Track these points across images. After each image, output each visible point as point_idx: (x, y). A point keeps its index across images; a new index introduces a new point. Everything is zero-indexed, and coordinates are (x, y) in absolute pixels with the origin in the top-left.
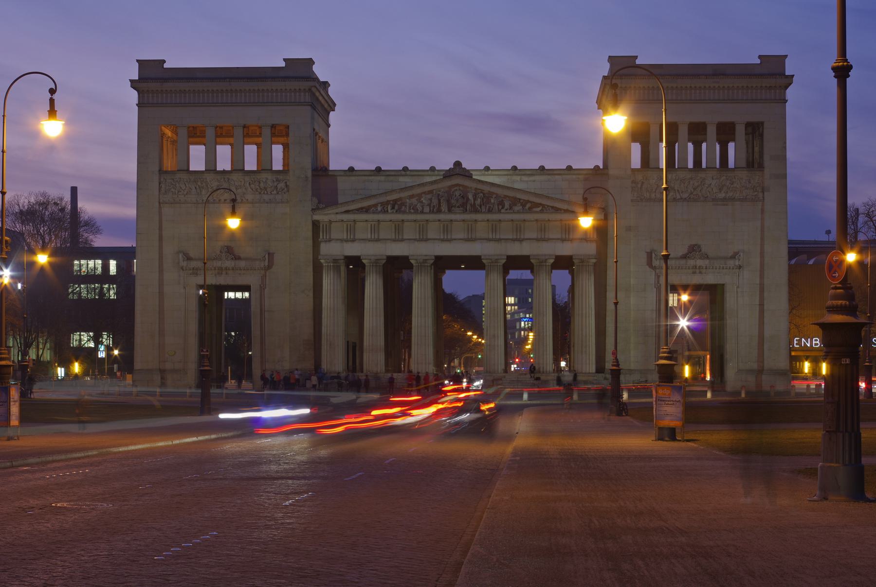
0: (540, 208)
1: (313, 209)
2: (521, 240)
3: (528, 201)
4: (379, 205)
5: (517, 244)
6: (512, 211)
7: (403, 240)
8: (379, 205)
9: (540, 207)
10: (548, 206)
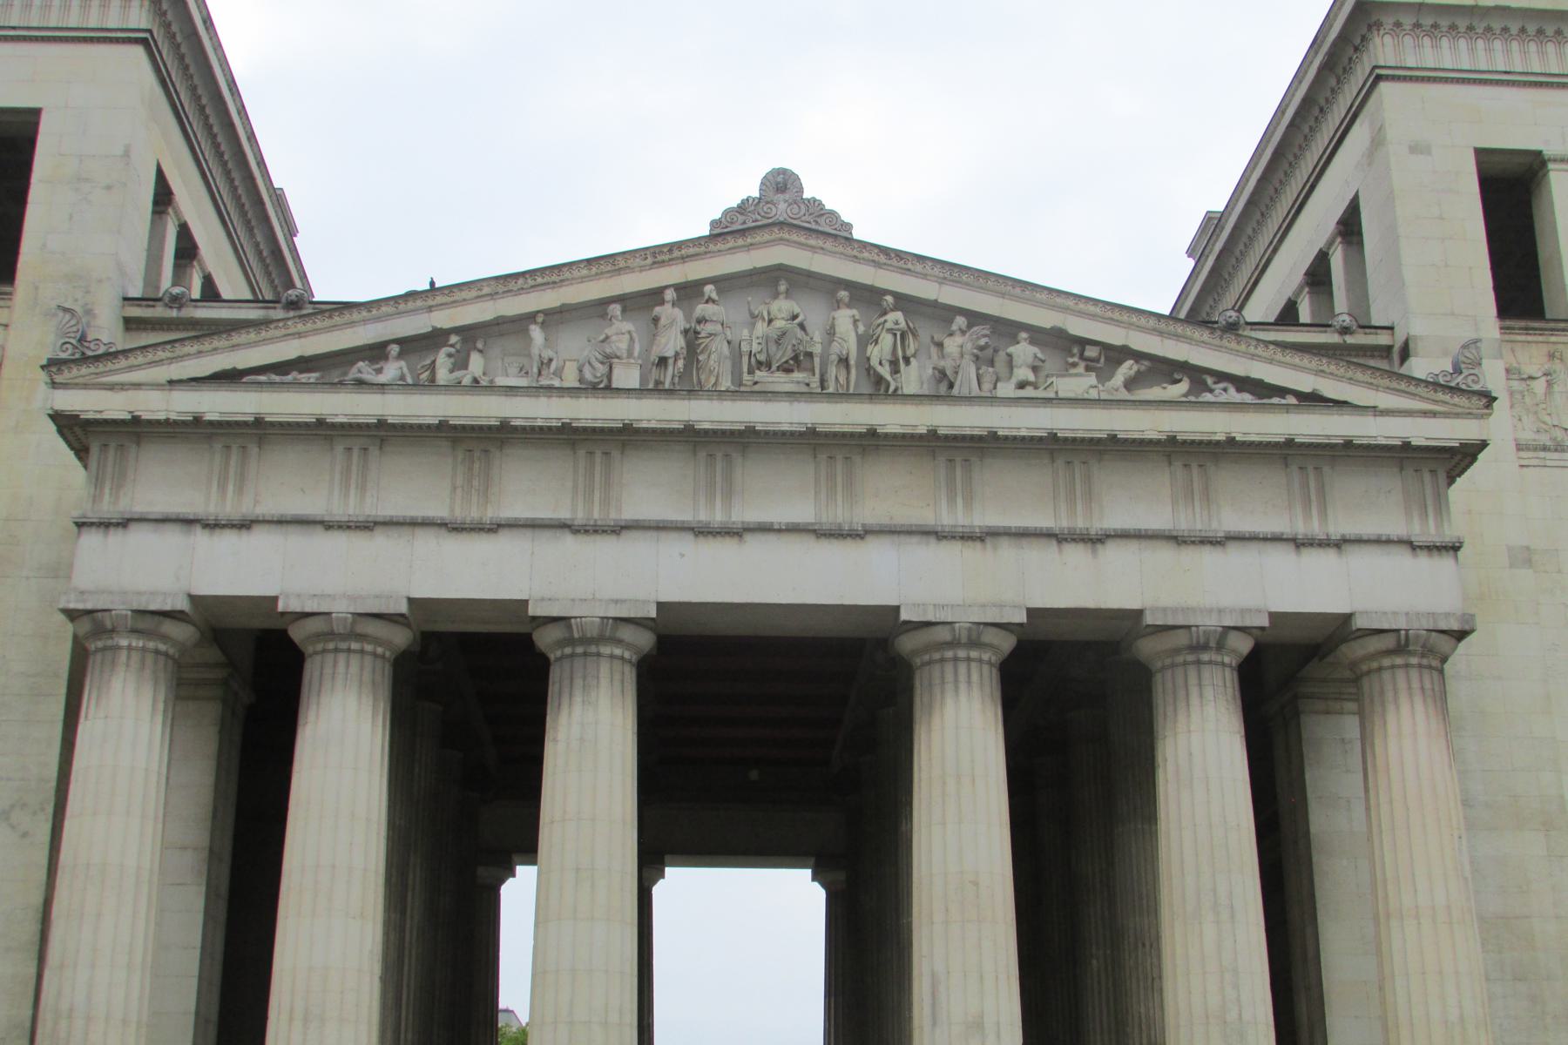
0: (1183, 387)
1: (53, 365)
2: (1095, 540)
3: (1123, 353)
4: (394, 349)
5: (1076, 555)
6: (1052, 395)
7: (495, 528)
8: (394, 349)
9: (1179, 381)
10: (1222, 377)
